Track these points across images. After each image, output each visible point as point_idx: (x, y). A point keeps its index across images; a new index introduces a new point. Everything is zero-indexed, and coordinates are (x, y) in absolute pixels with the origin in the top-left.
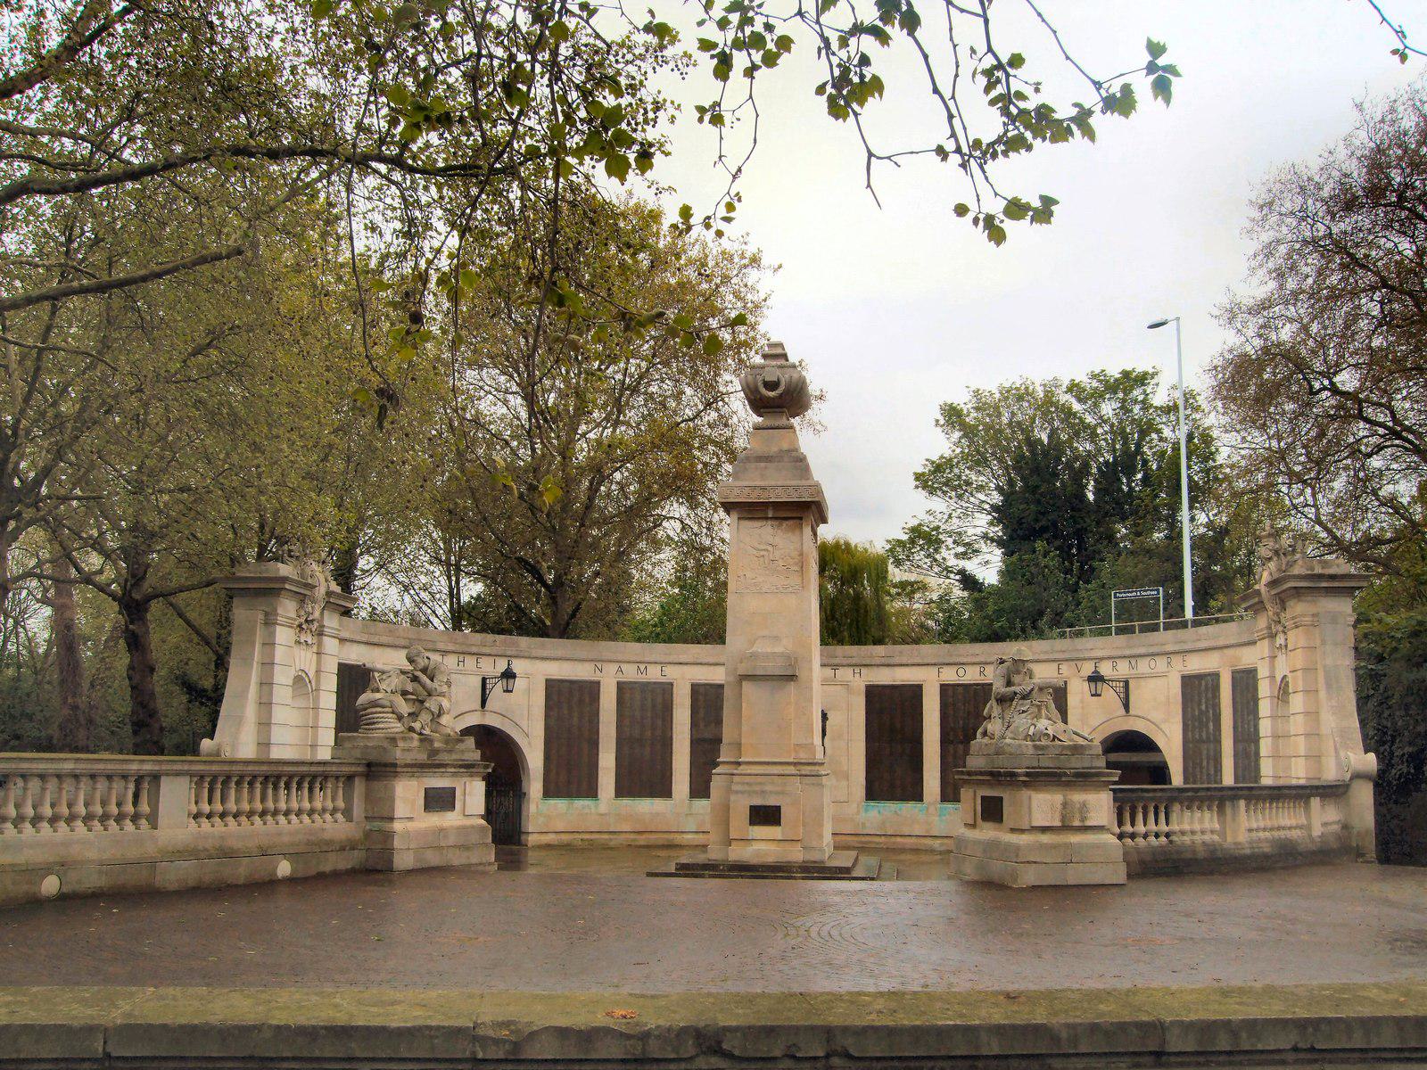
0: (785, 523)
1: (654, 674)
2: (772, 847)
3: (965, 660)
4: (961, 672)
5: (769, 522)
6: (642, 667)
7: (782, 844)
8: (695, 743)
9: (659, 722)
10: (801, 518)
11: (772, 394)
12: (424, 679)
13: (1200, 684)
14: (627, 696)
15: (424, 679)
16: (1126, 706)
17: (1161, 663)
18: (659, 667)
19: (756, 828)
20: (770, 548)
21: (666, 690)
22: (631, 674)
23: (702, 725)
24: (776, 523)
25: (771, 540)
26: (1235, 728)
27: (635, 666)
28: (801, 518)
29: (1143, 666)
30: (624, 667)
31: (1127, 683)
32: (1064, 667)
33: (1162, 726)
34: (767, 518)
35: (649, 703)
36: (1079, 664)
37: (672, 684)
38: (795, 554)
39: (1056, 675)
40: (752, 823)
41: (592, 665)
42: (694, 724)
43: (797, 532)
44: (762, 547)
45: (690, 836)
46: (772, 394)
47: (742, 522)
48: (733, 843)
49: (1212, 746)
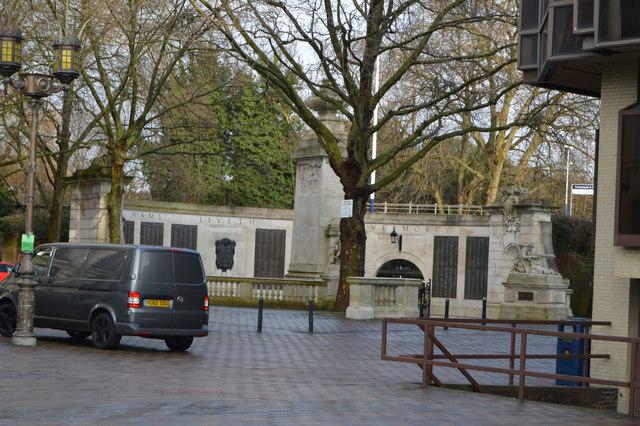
17: (422, 229)
29: (412, 229)
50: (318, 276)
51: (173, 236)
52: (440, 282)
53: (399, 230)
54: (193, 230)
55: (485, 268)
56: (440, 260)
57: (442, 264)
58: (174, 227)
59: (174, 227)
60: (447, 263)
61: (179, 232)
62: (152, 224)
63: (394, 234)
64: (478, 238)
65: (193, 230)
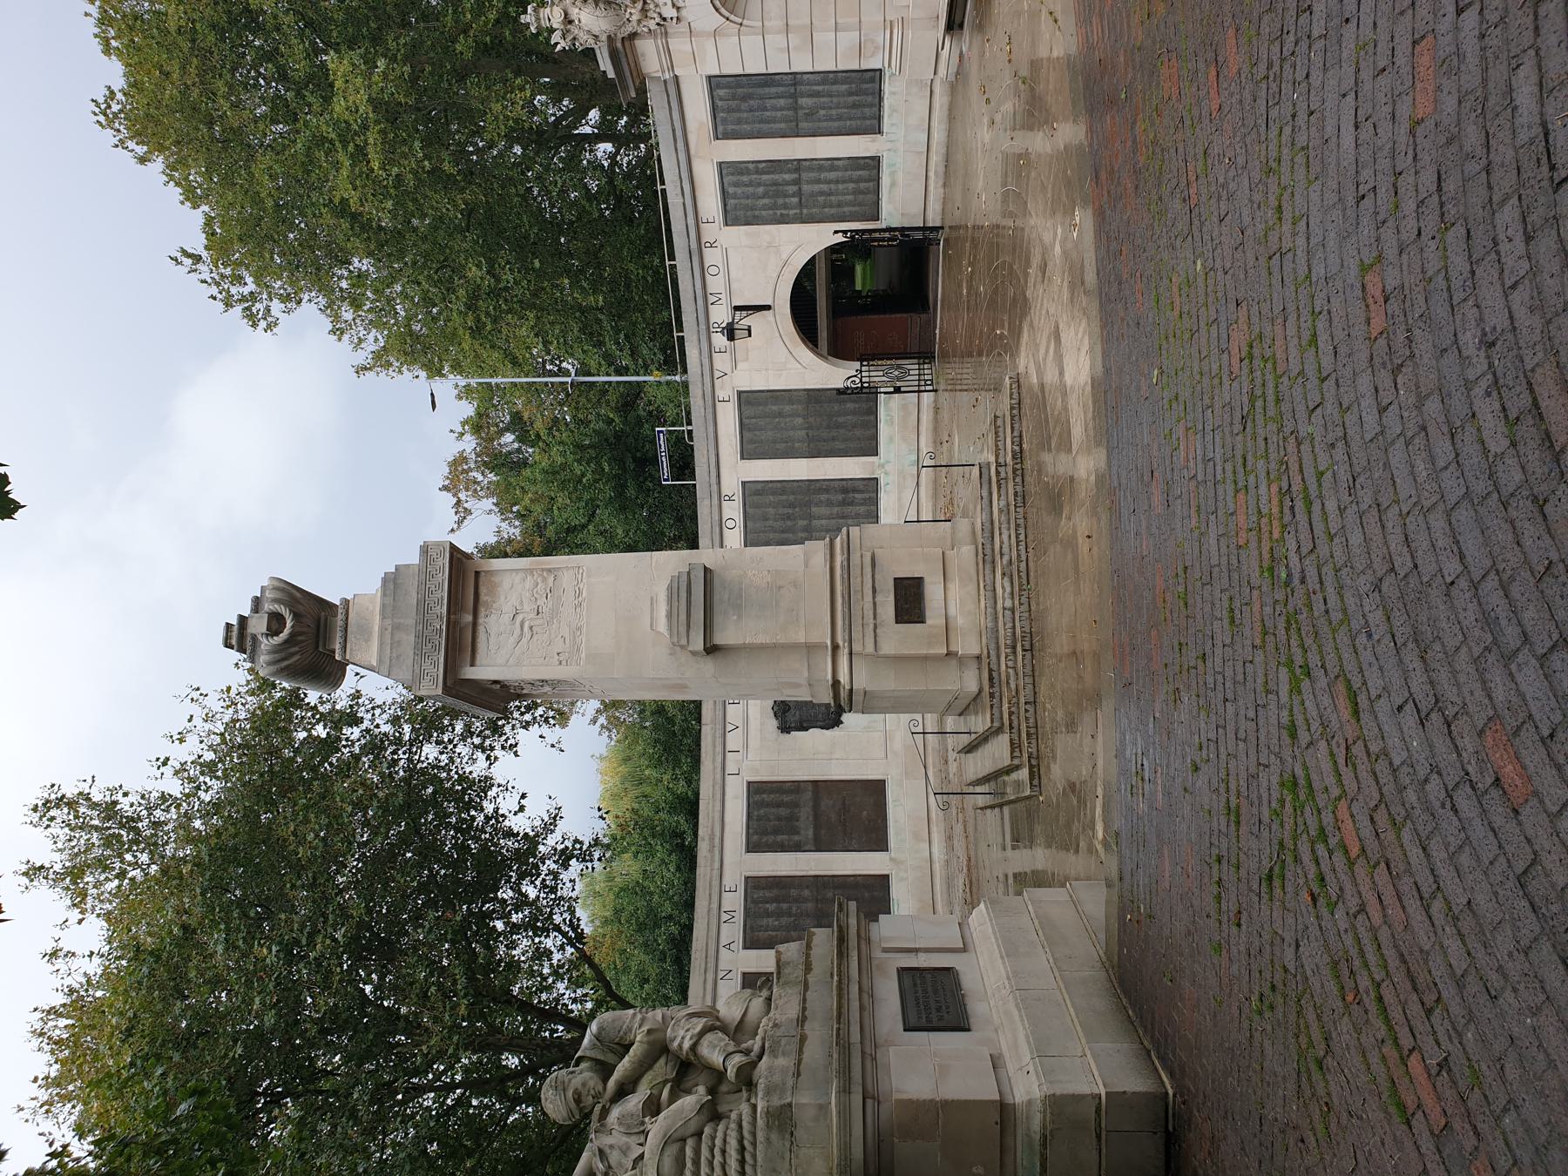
0: (483, 598)
1: (734, 901)
2: (954, 587)
3: (716, 518)
4: (730, 524)
5: (481, 620)
6: (725, 917)
7: (949, 575)
8: (820, 847)
9: (794, 892)
10: (477, 574)
11: (289, 624)
12: (624, 1066)
13: (735, 196)
14: (763, 935)
15: (624, 1066)
16: (768, 308)
17: (711, 256)
18: (724, 894)
19: (928, 613)
20: (519, 618)
21: (754, 885)
22: (733, 931)
23: (796, 838)
24: (482, 612)
25: (507, 618)
26: (784, 135)
27: (724, 926)
28: (477, 574)
29: (715, 284)
30: (723, 941)
31: (737, 308)
32: (720, 394)
33: (785, 257)
34: (475, 624)
35: (771, 907)
36: (717, 374)
37: (747, 878)
38: (529, 582)
39: (730, 405)
40: (920, 619)
41: (720, 982)
42: (797, 848)
43: (496, 579)
44: (518, 631)
45: (935, 850)
46: (289, 624)
47: (478, 662)
48: (953, 648)
49: (805, 176)
50: (1378, 768)
51: (783, 848)
52: (839, 205)
53: (720, 315)
54: (758, 792)
55: (795, 78)
56: (785, 206)
57: (795, 200)
58: (753, 847)
59: (753, 847)
60: (792, 189)
61: (765, 833)
62: (747, 913)
63: (730, 332)
64: (714, 110)
65: (758, 792)
